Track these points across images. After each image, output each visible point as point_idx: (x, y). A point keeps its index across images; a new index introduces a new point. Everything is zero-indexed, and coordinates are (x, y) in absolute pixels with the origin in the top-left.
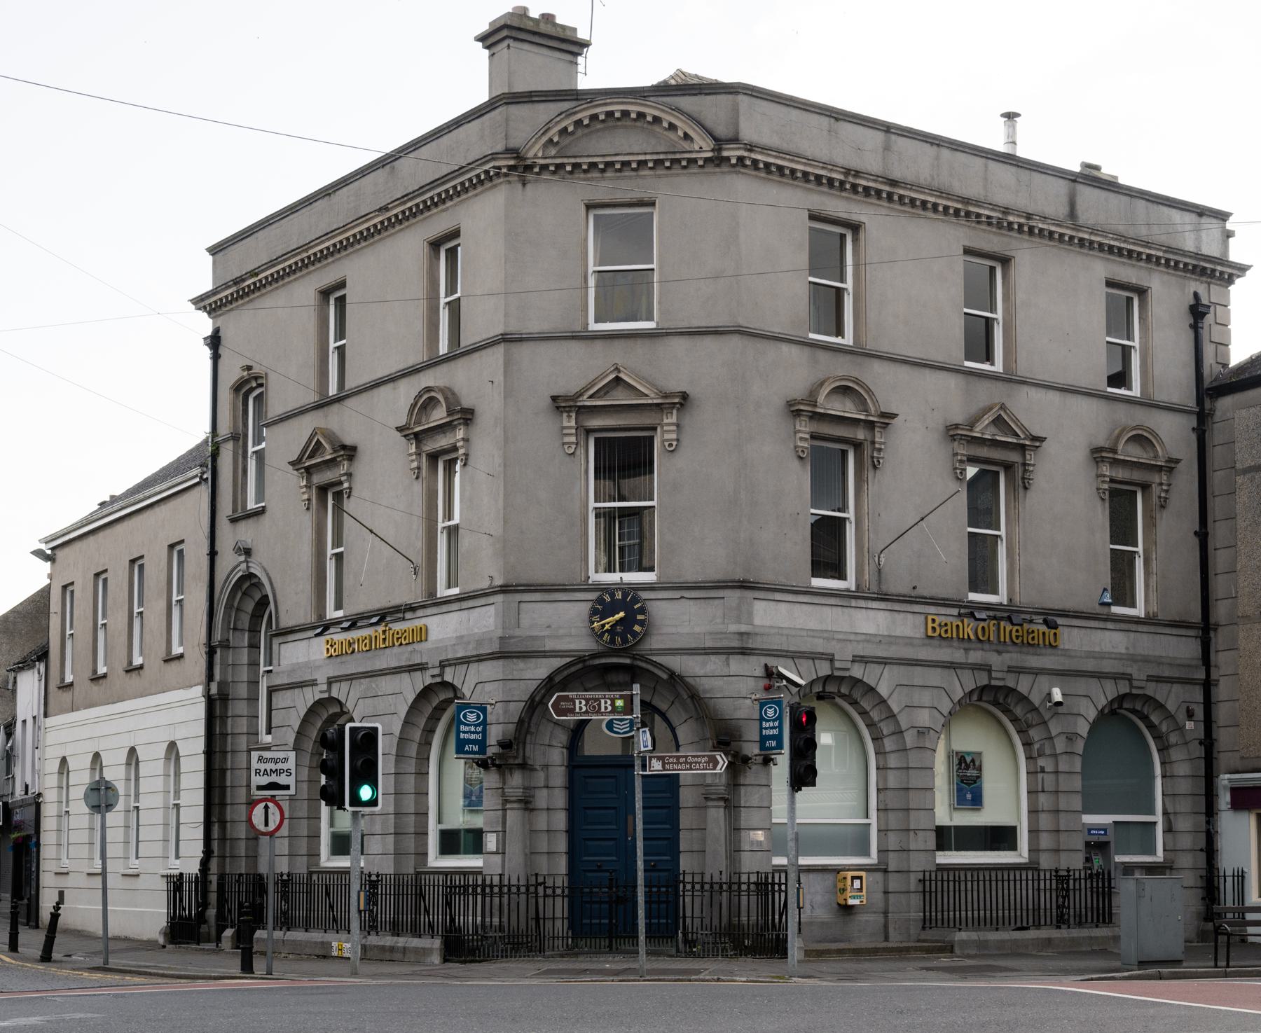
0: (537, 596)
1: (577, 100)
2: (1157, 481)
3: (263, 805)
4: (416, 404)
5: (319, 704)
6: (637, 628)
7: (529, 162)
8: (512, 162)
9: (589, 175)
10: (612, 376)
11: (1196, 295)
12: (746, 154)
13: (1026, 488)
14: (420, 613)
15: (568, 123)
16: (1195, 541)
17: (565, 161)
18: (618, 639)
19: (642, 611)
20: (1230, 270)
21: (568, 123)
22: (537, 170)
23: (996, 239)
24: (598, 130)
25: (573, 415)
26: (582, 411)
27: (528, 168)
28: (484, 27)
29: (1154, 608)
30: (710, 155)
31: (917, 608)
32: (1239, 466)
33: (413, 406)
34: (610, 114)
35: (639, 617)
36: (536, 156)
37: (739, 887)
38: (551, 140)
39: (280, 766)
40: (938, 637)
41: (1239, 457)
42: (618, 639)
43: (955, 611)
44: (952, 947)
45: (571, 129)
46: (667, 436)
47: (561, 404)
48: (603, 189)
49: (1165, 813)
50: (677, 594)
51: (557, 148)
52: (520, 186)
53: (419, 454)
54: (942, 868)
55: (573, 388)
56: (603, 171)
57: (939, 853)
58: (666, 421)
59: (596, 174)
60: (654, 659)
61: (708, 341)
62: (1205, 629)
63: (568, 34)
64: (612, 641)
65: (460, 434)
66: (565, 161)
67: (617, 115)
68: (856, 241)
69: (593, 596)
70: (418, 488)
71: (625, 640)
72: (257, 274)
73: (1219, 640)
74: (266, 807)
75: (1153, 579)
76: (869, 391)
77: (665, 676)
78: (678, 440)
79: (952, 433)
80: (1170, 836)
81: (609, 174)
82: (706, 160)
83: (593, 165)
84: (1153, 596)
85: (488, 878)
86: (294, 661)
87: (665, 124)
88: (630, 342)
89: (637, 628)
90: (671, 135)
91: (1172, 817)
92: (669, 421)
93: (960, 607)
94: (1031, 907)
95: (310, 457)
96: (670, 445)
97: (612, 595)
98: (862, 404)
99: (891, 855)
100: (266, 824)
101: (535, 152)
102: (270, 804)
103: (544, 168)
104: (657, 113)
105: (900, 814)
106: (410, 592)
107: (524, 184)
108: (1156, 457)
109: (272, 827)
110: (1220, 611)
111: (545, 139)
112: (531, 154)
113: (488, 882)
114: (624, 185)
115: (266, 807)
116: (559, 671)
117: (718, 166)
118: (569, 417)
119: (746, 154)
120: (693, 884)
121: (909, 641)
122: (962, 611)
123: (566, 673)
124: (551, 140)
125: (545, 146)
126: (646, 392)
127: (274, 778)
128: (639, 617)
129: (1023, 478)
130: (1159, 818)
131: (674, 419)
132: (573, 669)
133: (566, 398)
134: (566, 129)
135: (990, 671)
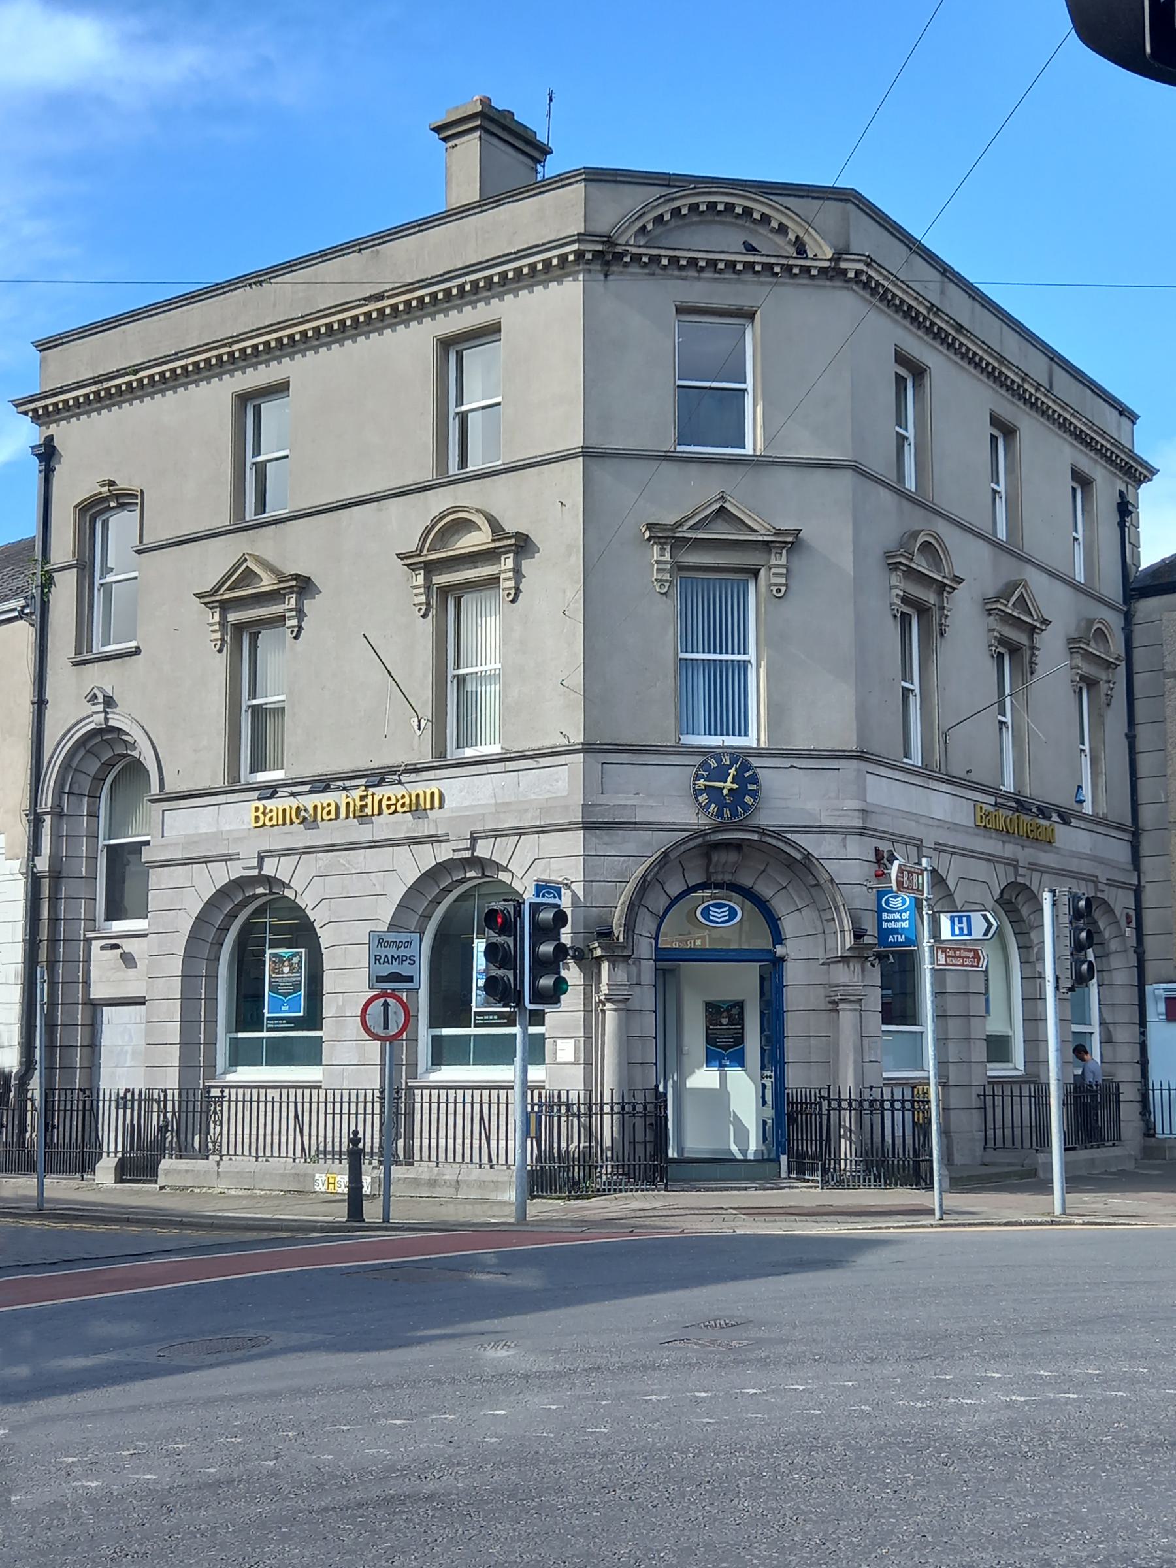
0: (624, 758)
1: (668, 186)
2: (1104, 678)
3: (382, 1000)
4: (433, 526)
5: (239, 884)
6: (748, 799)
7: (619, 249)
8: (600, 247)
9: (684, 274)
10: (716, 506)
11: (1121, 493)
12: (865, 268)
13: (1032, 673)
14: (425, 775)
15: (665, 210)
16: (1125, 743)
17: (663, 252)
18: (727, 812)
19: (754, 779)
20: (1145, 473)
21: (665, 210)
22: (627, 259)
23: (1008, 406)
24: (693, 224)
25: (668, 548)
26: (679, 544)
27: (619, 256)
28: (499, 104)
29: (1103, 809)
30: (827, 264)
31: (970, 794)
32: (1168, 668)
33: (428, 531)
34: (712, 206)
35: (750, 787)
36: (627, 244)
37: (882, 1105)
38: (644, 227)
39: (402, 952)
40: (984, 825)
41: (1168, 659)
42: (727, 812)
43: (992, 800)
44: (1036, 1170)
45: (685, 211)
46: (774, 580)
47: (661, 535)
48: (698, 291)
49: (1102, 1023)
50: (786, 763)
51: (647, 239)
52: (602, 277)
53: (428, 587)
54: (994, 1082)
55: (670, 519)
56: (702, 269)
57: (989, 1065)
58: (773, 562)
59: (692, 273)
60: (788, 835)
61: (820, 472)
62: (1135, 834)
63: (529, 136)
64: (720, 814)
65: (508, 562)
66: (663, 252)
67: (720, 207)
68: (918, 385)
69: (699, 760)
70: (426, 627)
71: (734, 814)
72: (136, 372)
73: (1147, 845)
74: (386, 1005)
75: (1102, 781)
76: (945, 550)
77: (799, 856)
78: (786, 585)
79: (989, 607)
80: (1108, 1047)
81: (708, 274)
82: (822, 270)
83: (693, 262)
84: (1102, 797)
85: (564, 1094)
86: (191, 831)
87: (775, 225)
88: (730, 469)
89: (748, 799)
90: (778, 239)
91: (1111, 1027)
92: (778, 562)
93: (996, 795)
94: (1026, 1123)
95: (229, 589)
96: (779, 591)
97: (719, 761)
98: (937, 563)
99: (951, 1067)
100: (386, 1027)
101: (628, 240)
102: (389, 1000)
103: (636, 258)
104: (767, 211)
105: (958, 1021)
106: (423, 753)
107: (606, 276)
108: (1107, 652)
109: (393, 1031)
110: (1148, 815)
111: (639, 224)
112: (622, 241)
113: (564, 1098)
114: (721, 288)
115: (386, 1005)
116: (676, 845)
117: (831, 279)
118: (663, 549)
119: (865, 268)
120: (892, 1101)
121: (954, 827)
122: (999, 800)
123: (682, 848)
124: (644, 227)
125: (636, 234)
126: (755, 527)
127: (395, 968)
128: (750, 787)
129: (1031, 663)
130: (1096, 1028)
131: (783, 561)
132: (691, 844)
133: (664, 528)
134: (679, 209)
135: (1016, 867)
